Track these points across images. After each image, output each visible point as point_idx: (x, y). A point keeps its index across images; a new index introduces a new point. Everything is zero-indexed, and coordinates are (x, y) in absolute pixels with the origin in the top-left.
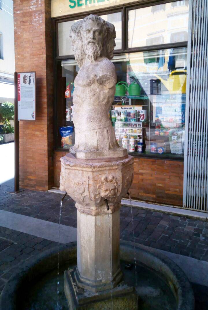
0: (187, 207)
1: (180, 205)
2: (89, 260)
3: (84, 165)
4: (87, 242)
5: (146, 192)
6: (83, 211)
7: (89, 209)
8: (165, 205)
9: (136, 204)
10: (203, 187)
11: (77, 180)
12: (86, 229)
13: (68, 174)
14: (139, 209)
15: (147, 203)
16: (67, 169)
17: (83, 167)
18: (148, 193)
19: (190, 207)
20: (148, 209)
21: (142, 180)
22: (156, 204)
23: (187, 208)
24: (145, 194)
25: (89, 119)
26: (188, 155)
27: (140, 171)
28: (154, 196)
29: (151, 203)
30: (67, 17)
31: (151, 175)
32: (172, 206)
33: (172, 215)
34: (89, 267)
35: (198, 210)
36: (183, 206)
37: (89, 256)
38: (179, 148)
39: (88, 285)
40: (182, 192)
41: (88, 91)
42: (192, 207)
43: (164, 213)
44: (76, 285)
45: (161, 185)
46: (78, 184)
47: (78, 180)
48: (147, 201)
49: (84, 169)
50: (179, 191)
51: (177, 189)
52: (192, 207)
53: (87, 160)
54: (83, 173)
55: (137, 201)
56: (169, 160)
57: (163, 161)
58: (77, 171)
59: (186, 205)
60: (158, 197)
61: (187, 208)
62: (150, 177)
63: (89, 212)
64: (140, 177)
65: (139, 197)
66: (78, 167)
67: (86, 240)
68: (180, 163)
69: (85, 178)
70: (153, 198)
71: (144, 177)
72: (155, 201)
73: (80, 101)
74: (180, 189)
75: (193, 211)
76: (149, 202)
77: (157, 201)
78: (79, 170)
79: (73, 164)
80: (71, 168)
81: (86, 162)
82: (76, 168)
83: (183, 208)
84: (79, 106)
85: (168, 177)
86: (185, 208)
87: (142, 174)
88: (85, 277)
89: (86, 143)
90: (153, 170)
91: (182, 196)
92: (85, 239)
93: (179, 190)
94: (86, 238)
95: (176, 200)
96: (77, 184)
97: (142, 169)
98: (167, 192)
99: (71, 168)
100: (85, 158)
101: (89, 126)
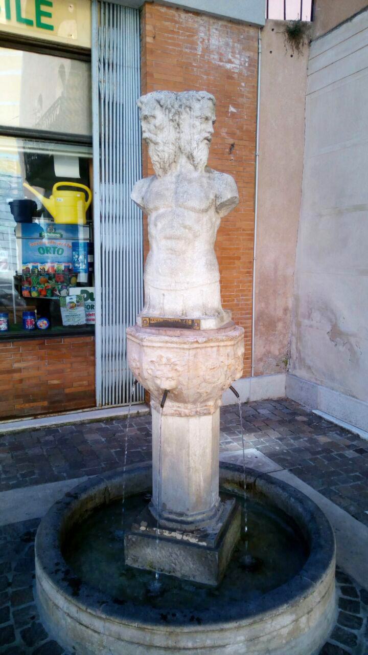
0: (102, 405)
1: (92, 404)
2: (202, 484)
3: (224, 338)
4: (200, 458)
5: (29, 401)
6: (196, 412)
7: (206, 406)
8: (68, 413)
9: (20, 426)
10: (109, 371)
11: (210, 364)
12: (198, 439)
13: (193, 357)
14: (30, 432)
15: (35, 418)
16: (194, 348)
17: (223, 341)
18: (34, 401)
19: (108, 404)
20: (46, 426)
21: (21, 381)
22: (51, 415)
23: (103, 407)
24: (27, 405)
25: (209, 266)
26: (102, 324)
27: (16, 365)
28: (46, 403)
29: (43, 416)
30: (61, 47)
31: (38, 369)
32: (81, 411)
33: (89, 423)
34: (202, 491)
35: (119, 405)
36: (97, 405)
37: (202, 478)
38: (80, 315)
39: (203, 520)
40: (93, 382)
41: (205, 219)
42: (110, 403)
43: (74, 424)
44: (182, 532)
45: (56, 382)
46: (214, 368)
47: (212, 363)
48: (35, 416)
49: (222, 344)
50: (87, 384)
51: (85, 382)
52: (110, 403)
53: (219, 330)
54: (218, 350)
55: (17, 420)
56: (69, 337)
57: (59, 340)
58: (209, 349)
59: (101, 403)
60: (51, 403)
61: (103, 407)
62: (33, 373)
63: (205, 412)
64: (17, 376)
65: (15, 413)
66: (214, 342)
67: (197, 455)
68: (88, 339)
69: (223, 357)
70: (44, 408)
71: (25, 374)
72: (47, 411)
73: (190, 236)
74: (88, 381)
75: (113, 409)
76: (39, 417)
77: (51, 411)
78: (212, 347)
79: (204, 340)
80: (199, 346)
81: (218, 333)
82: (208, 345)
83: (96, 408)
84: (187, 243)
85: (69, 365)
86: (100, 408)
87: (19, 370)
88: (195, 513)
89: (203, 305)
90: (42, 358)
91: (94, 391)
92: (196, 455)
93: (87, 382)
94: (197, 453)
95: (87, 399)
96: (211, 369)
97: (19, 361)
98: (67, 391)
99: (199, 346)
100: (215, 328)
101: (209, 277)
